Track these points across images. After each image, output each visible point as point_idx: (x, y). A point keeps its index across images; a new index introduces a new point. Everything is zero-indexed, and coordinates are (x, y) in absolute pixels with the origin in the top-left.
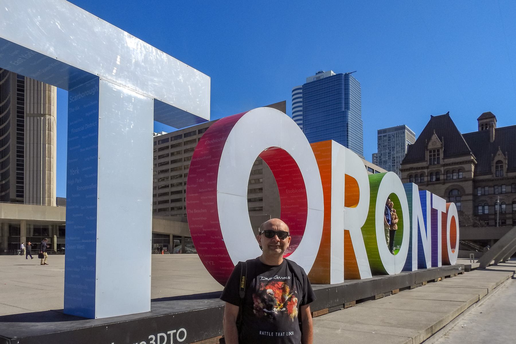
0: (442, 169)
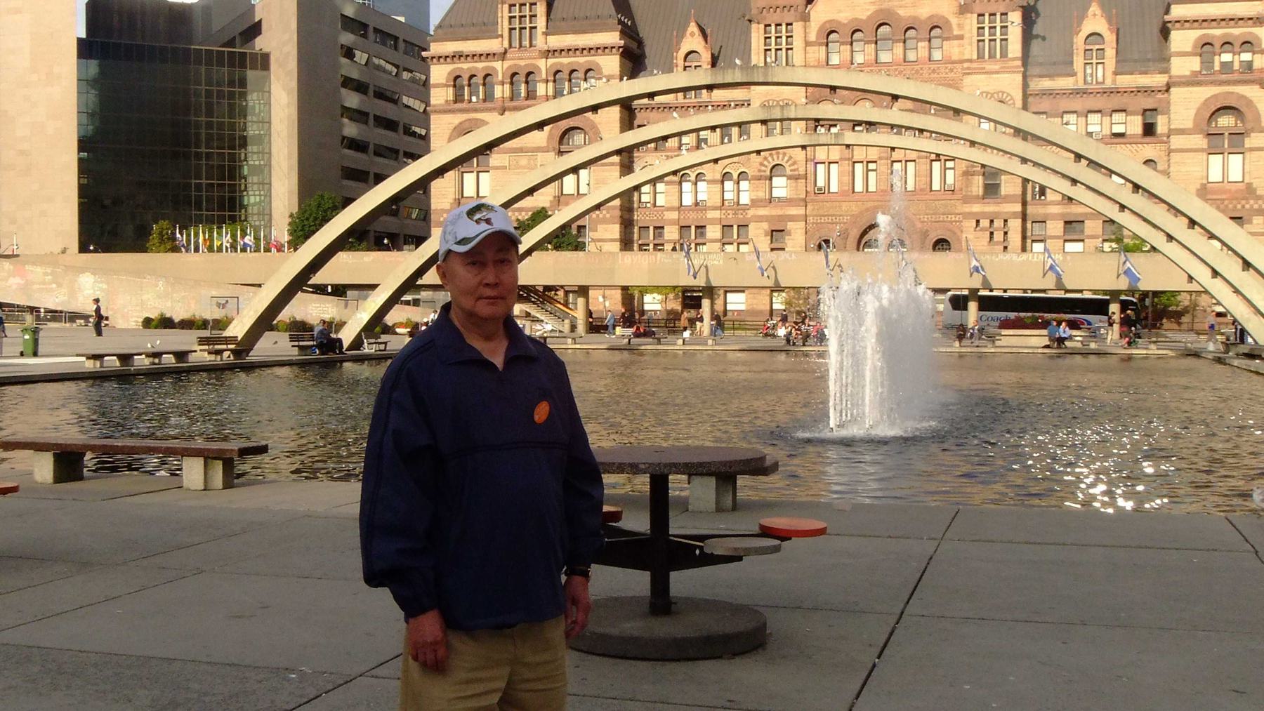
0: (542, 64)
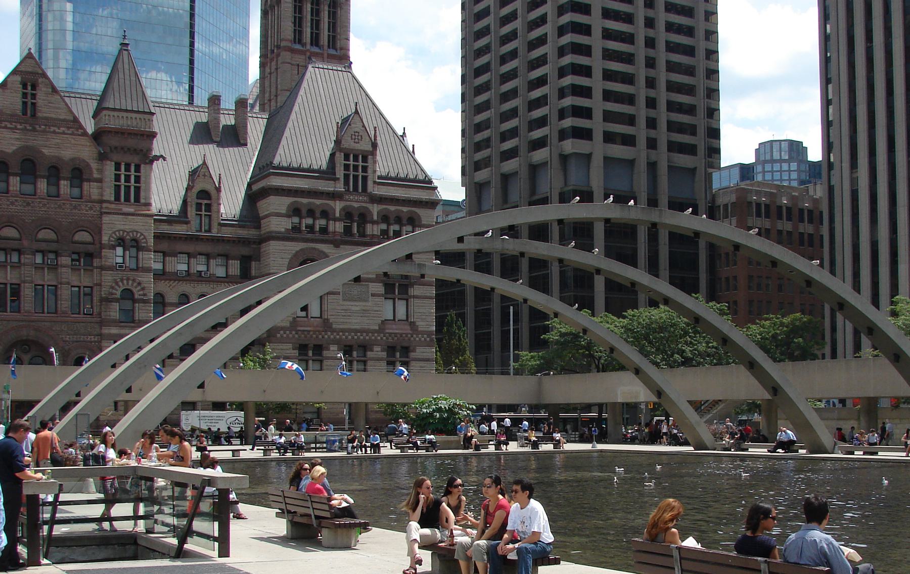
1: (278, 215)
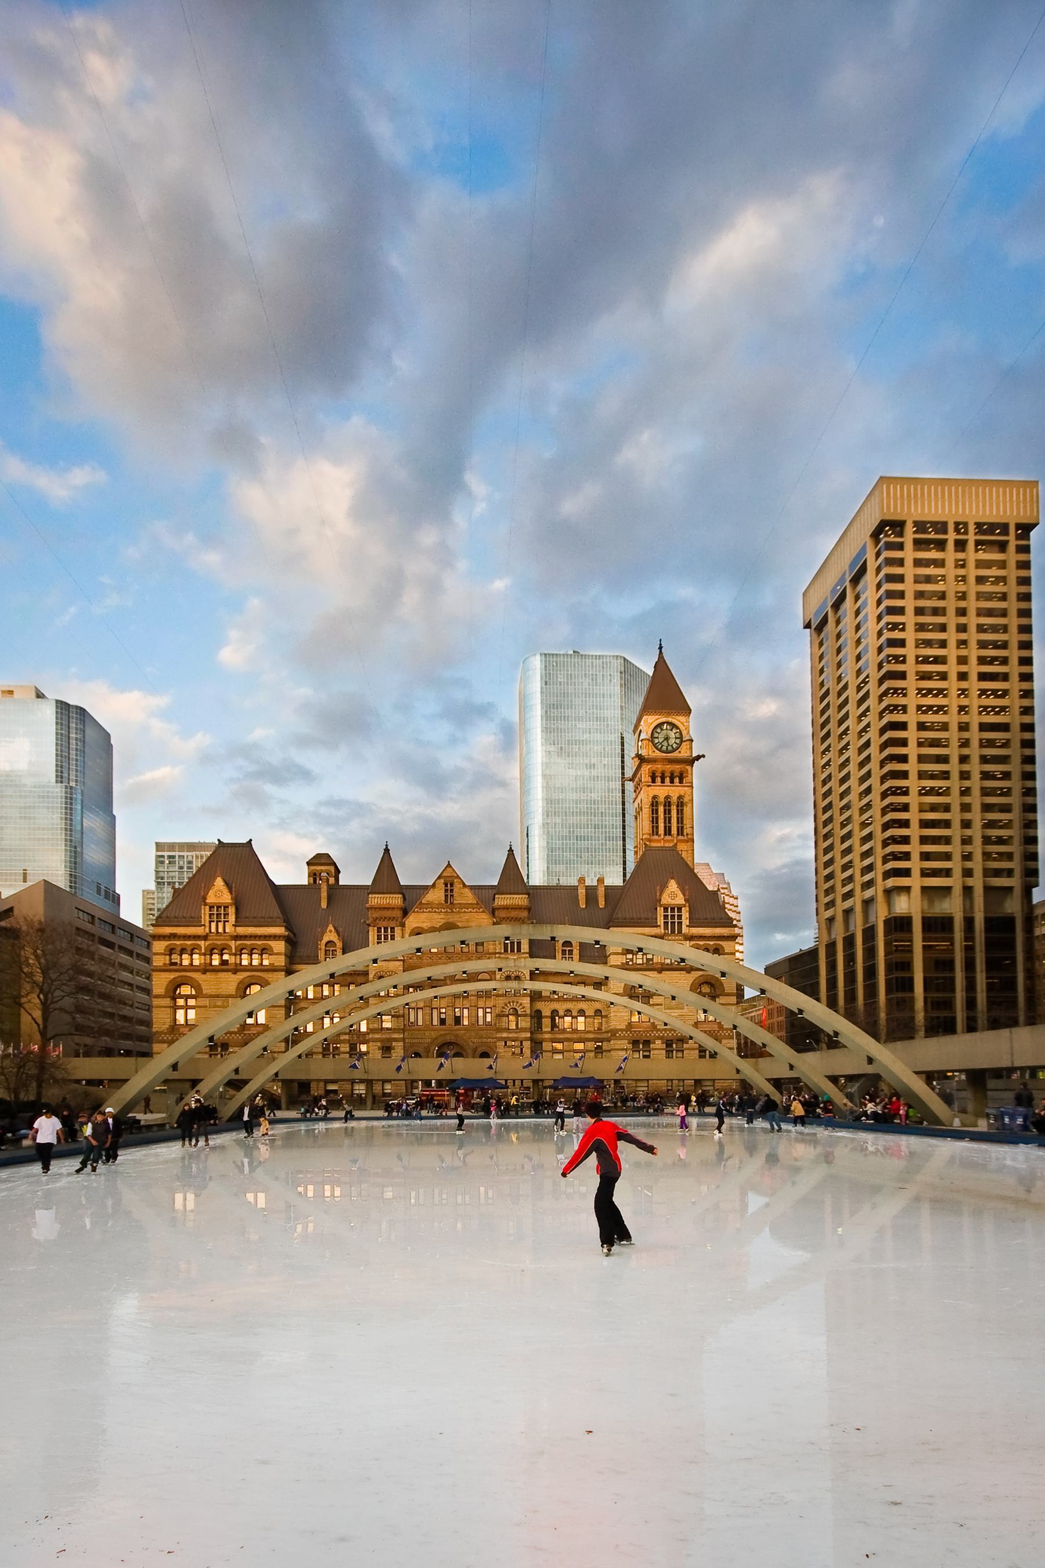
0: (232, 944)
1: (618, 954)
